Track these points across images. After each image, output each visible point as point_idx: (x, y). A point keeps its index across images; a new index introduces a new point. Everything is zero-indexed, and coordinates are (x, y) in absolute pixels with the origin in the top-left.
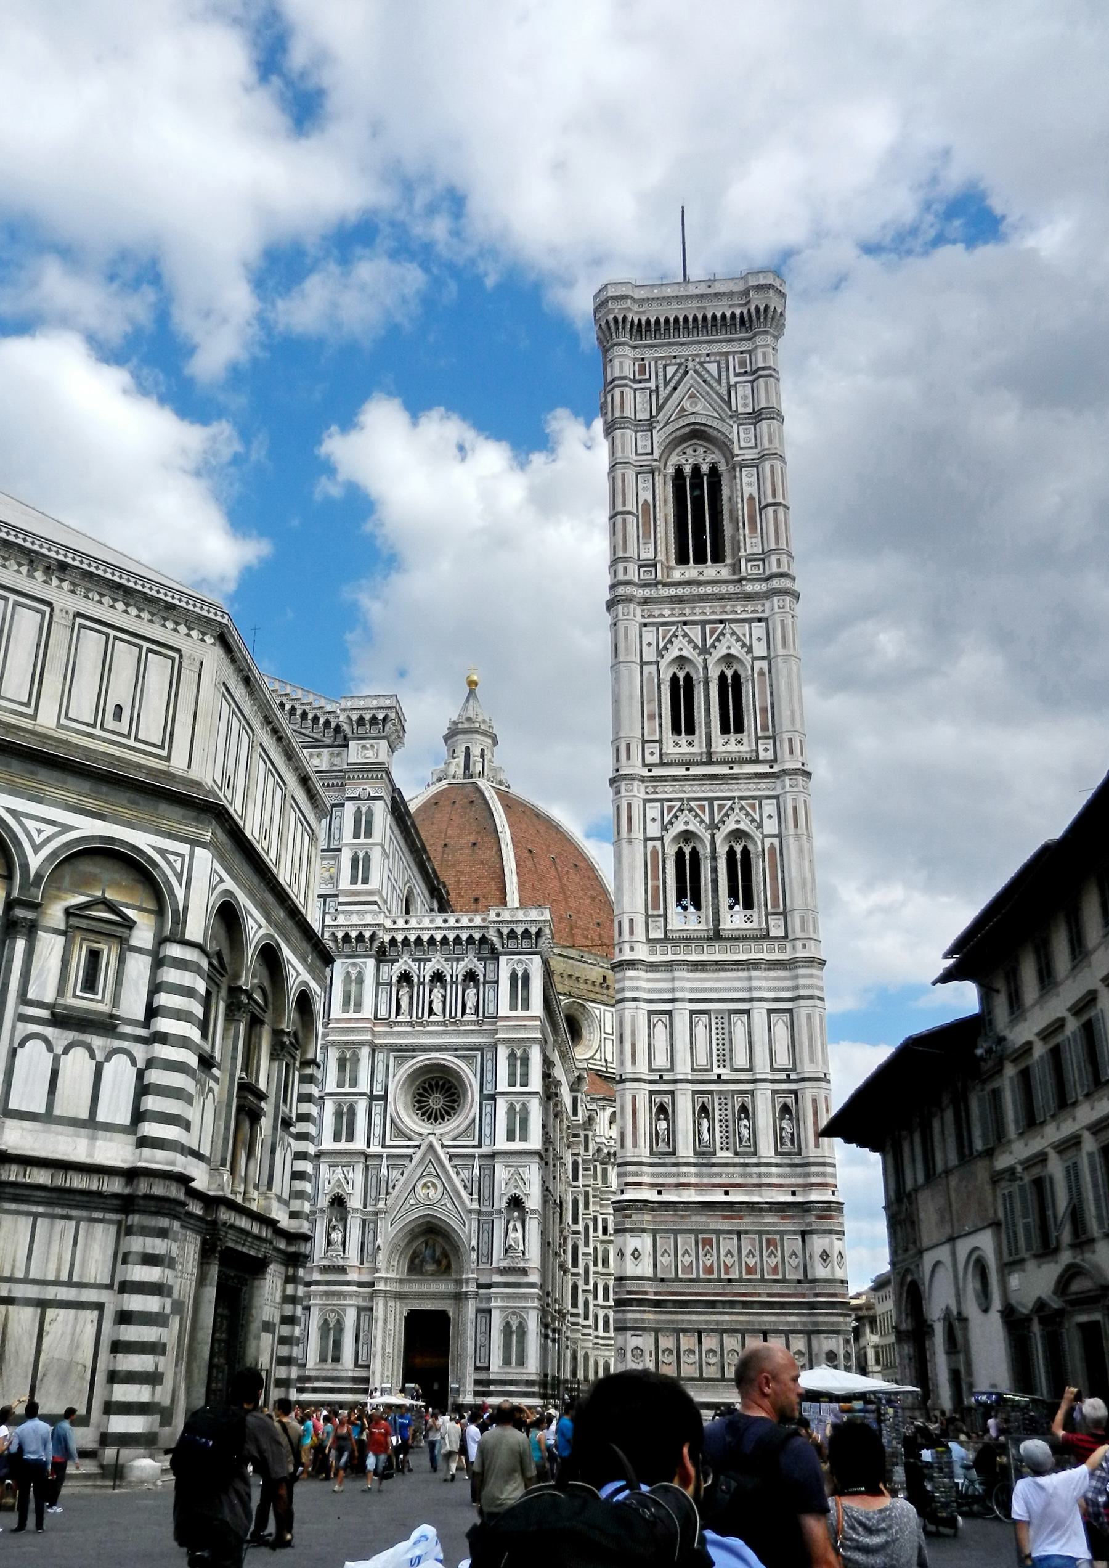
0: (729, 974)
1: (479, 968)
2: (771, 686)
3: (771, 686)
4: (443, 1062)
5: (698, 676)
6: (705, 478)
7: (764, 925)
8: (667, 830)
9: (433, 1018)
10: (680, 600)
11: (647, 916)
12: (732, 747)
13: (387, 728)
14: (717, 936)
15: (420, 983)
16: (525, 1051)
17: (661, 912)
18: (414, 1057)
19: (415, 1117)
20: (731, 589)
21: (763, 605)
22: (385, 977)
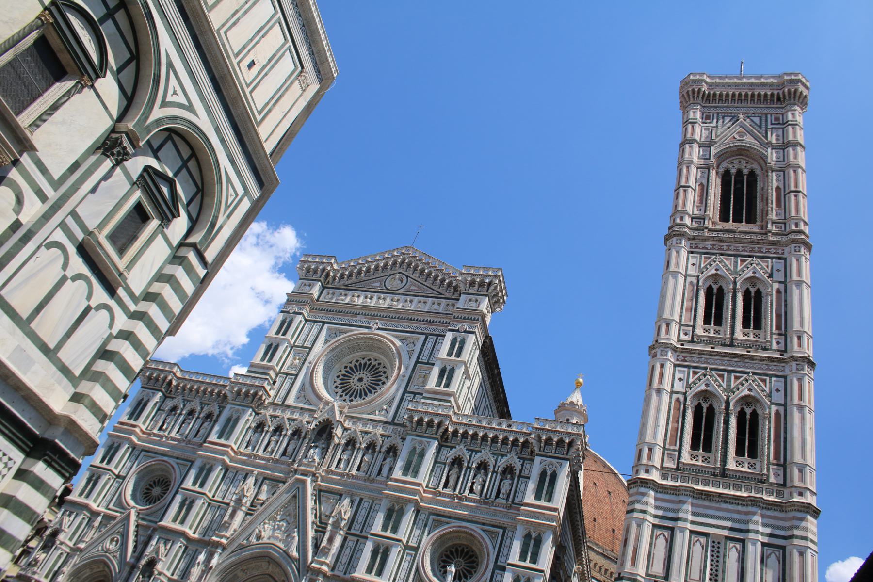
0: (730, 507)
1: (518, 465)
2: (786, 301)
3: (786, 301)
4: (470, 531)
5: (728, 288)
6: (745, 177)
7: (765, 472)
8: (691, 388)
9: (472, 496)
10: (720, 240)
11: (664, 448)
12: (751, 338)
13: (490, 291)
14: (724, 473)
15: (468, 467)
16: (539, 535)
17: (677, 448)
18: (448, 523)
19: (437, 572)
20: (759, 237)
21: (783, 250)
22: (443, 458)
